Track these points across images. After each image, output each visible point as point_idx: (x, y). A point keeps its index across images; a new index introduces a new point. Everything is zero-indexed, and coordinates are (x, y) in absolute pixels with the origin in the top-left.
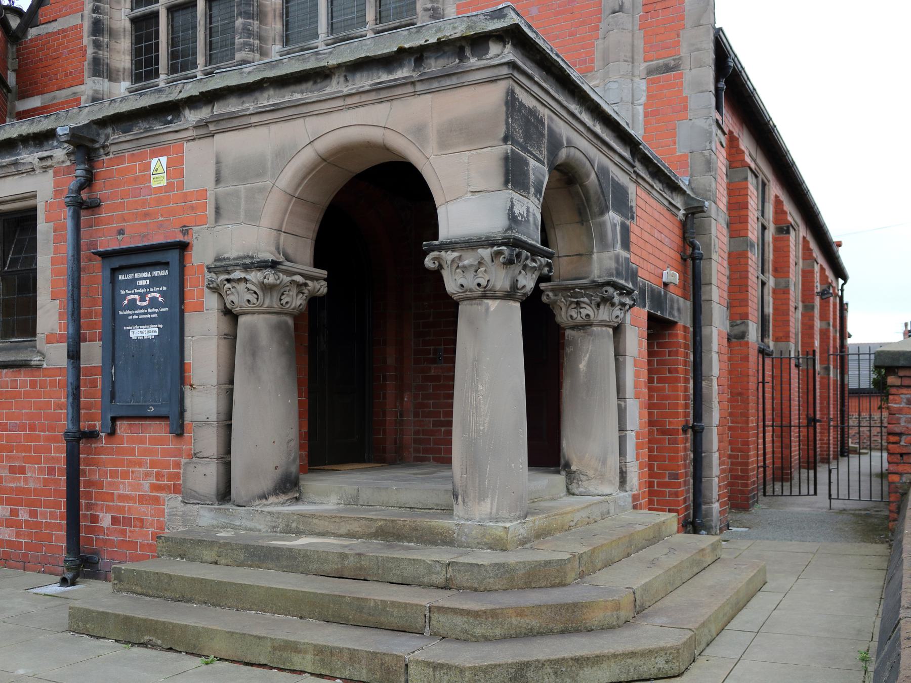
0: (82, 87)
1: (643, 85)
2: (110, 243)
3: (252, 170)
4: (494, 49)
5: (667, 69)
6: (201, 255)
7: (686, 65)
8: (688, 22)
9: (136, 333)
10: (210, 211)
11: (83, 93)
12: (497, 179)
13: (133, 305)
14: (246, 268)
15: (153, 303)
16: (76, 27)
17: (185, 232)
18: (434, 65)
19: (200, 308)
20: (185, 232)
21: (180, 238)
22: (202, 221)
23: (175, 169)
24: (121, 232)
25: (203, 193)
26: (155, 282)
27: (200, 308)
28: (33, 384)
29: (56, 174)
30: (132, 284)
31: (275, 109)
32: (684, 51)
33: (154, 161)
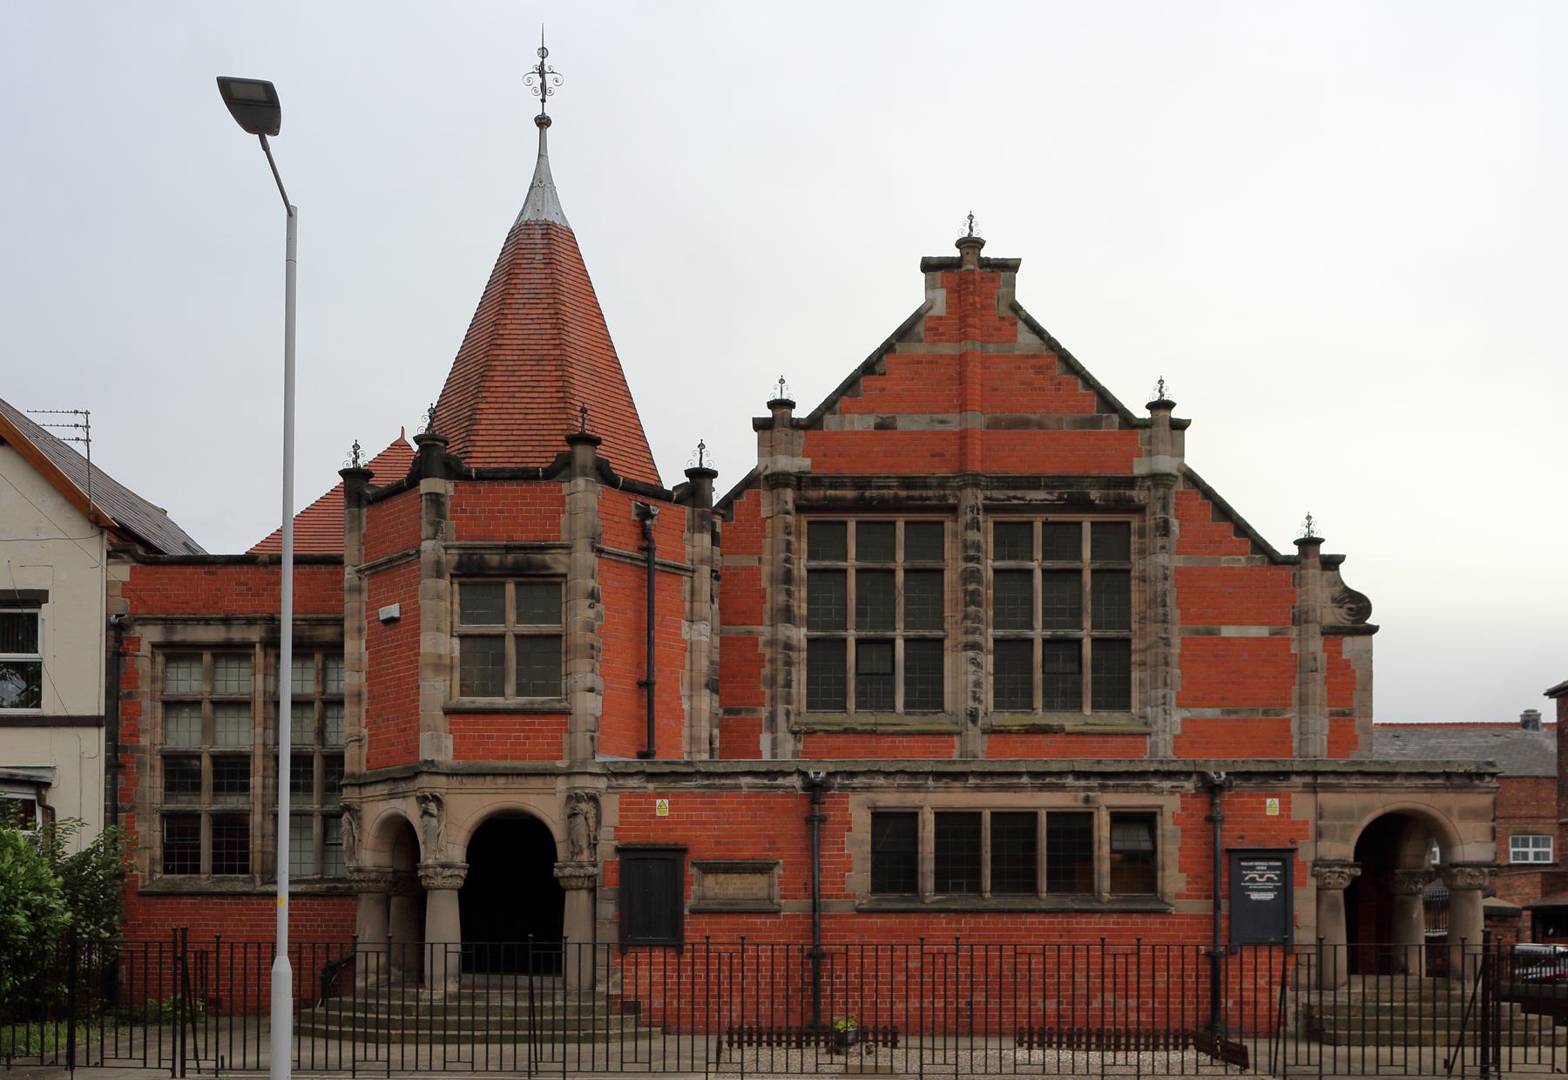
0: (761, 628)
1: (1326, 722)
2: (1228, 838)
3: (1341, 815)
4: (1487, 779)
5: (1344, 714)
6: (1306, 854)
7: (1357, 714)
8: (1358, 687)
9: (1255, 896)
10: (1311, 833)
11: (761, 634)
12: (1489, 838)
13: (1253, 880)
14: (1343, 866)
15: (1270, 880)
16: (751, 568)
17: (1292, 842)
18: (1457, 781)
19: (1304, 884)
20: (1292, 842)
21: (1290, 846)
22: (1306, 837)
23: (1286, 805)
24: (1242, 837)
25: (1306, 823)
26: (1270, 868)
27: (1304, 884)
28: (1162, 923)
29: (1183, 796)
30: (1253, 868)
31: (1366, 786)
32: (1355, 705)
33: (1269, 801)
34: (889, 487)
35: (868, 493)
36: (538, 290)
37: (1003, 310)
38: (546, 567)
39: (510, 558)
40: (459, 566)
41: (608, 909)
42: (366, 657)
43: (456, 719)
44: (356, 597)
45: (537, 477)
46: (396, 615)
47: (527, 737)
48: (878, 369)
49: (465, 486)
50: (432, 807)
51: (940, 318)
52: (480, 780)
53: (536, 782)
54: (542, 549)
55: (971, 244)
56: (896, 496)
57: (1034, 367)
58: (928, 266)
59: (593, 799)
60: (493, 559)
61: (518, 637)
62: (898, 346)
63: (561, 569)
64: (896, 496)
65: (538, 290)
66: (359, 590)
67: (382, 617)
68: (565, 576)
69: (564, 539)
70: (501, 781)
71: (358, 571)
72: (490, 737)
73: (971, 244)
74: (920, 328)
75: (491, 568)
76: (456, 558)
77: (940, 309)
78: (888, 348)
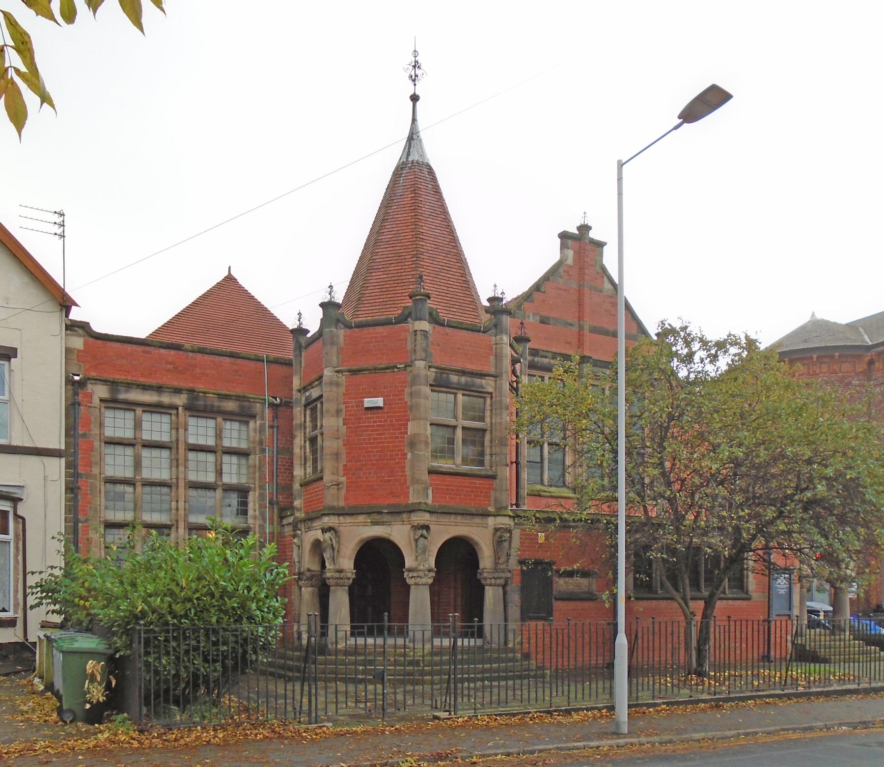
34: (546, 357)
35: (536, 359)
36: (412, 207)
37: (598, 269)
38: (482, 387)
39: (463, 379)
40: (435, 380)
41: (515, 598)
42: (344, 429)
43: (435, 477)
44: (335, 389)
45: (479, 331)
46: (381, 405)
47: (472, 492)
48: (542, 289)
49: (439, 328)
50: (425, 532)
51: (570, 266)
52: (448, 516)
53: (477, 520)
54: (482, 375)
55: (584, 229)
56: (549, 363)
57: (611, 303)
58: (564, 236)
59: (510, 531)
60: (454, 378)
61: (464, 428)
62: (551, 278)
63: (491, 390)
64: (549, 363)
65: (412, 207)
66: (338, 384)
67: (366, 405)
68: (491, 393)
69: (492, 371)
70: (459, 518)
71: (337, 372)
72: (452, 490)
73: (584, 229)
74: (561, 270)
75: (453, 383)
76: (434, 374)
77: (570, 261)
78: (546, 278)
